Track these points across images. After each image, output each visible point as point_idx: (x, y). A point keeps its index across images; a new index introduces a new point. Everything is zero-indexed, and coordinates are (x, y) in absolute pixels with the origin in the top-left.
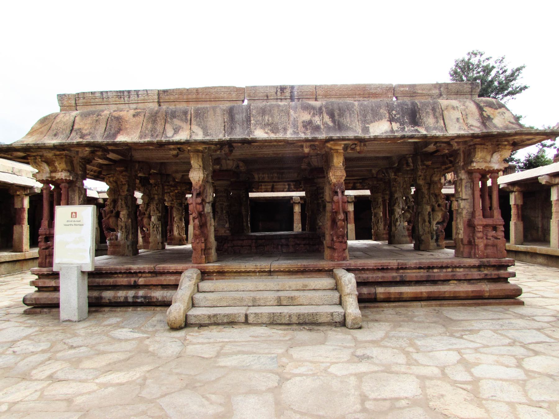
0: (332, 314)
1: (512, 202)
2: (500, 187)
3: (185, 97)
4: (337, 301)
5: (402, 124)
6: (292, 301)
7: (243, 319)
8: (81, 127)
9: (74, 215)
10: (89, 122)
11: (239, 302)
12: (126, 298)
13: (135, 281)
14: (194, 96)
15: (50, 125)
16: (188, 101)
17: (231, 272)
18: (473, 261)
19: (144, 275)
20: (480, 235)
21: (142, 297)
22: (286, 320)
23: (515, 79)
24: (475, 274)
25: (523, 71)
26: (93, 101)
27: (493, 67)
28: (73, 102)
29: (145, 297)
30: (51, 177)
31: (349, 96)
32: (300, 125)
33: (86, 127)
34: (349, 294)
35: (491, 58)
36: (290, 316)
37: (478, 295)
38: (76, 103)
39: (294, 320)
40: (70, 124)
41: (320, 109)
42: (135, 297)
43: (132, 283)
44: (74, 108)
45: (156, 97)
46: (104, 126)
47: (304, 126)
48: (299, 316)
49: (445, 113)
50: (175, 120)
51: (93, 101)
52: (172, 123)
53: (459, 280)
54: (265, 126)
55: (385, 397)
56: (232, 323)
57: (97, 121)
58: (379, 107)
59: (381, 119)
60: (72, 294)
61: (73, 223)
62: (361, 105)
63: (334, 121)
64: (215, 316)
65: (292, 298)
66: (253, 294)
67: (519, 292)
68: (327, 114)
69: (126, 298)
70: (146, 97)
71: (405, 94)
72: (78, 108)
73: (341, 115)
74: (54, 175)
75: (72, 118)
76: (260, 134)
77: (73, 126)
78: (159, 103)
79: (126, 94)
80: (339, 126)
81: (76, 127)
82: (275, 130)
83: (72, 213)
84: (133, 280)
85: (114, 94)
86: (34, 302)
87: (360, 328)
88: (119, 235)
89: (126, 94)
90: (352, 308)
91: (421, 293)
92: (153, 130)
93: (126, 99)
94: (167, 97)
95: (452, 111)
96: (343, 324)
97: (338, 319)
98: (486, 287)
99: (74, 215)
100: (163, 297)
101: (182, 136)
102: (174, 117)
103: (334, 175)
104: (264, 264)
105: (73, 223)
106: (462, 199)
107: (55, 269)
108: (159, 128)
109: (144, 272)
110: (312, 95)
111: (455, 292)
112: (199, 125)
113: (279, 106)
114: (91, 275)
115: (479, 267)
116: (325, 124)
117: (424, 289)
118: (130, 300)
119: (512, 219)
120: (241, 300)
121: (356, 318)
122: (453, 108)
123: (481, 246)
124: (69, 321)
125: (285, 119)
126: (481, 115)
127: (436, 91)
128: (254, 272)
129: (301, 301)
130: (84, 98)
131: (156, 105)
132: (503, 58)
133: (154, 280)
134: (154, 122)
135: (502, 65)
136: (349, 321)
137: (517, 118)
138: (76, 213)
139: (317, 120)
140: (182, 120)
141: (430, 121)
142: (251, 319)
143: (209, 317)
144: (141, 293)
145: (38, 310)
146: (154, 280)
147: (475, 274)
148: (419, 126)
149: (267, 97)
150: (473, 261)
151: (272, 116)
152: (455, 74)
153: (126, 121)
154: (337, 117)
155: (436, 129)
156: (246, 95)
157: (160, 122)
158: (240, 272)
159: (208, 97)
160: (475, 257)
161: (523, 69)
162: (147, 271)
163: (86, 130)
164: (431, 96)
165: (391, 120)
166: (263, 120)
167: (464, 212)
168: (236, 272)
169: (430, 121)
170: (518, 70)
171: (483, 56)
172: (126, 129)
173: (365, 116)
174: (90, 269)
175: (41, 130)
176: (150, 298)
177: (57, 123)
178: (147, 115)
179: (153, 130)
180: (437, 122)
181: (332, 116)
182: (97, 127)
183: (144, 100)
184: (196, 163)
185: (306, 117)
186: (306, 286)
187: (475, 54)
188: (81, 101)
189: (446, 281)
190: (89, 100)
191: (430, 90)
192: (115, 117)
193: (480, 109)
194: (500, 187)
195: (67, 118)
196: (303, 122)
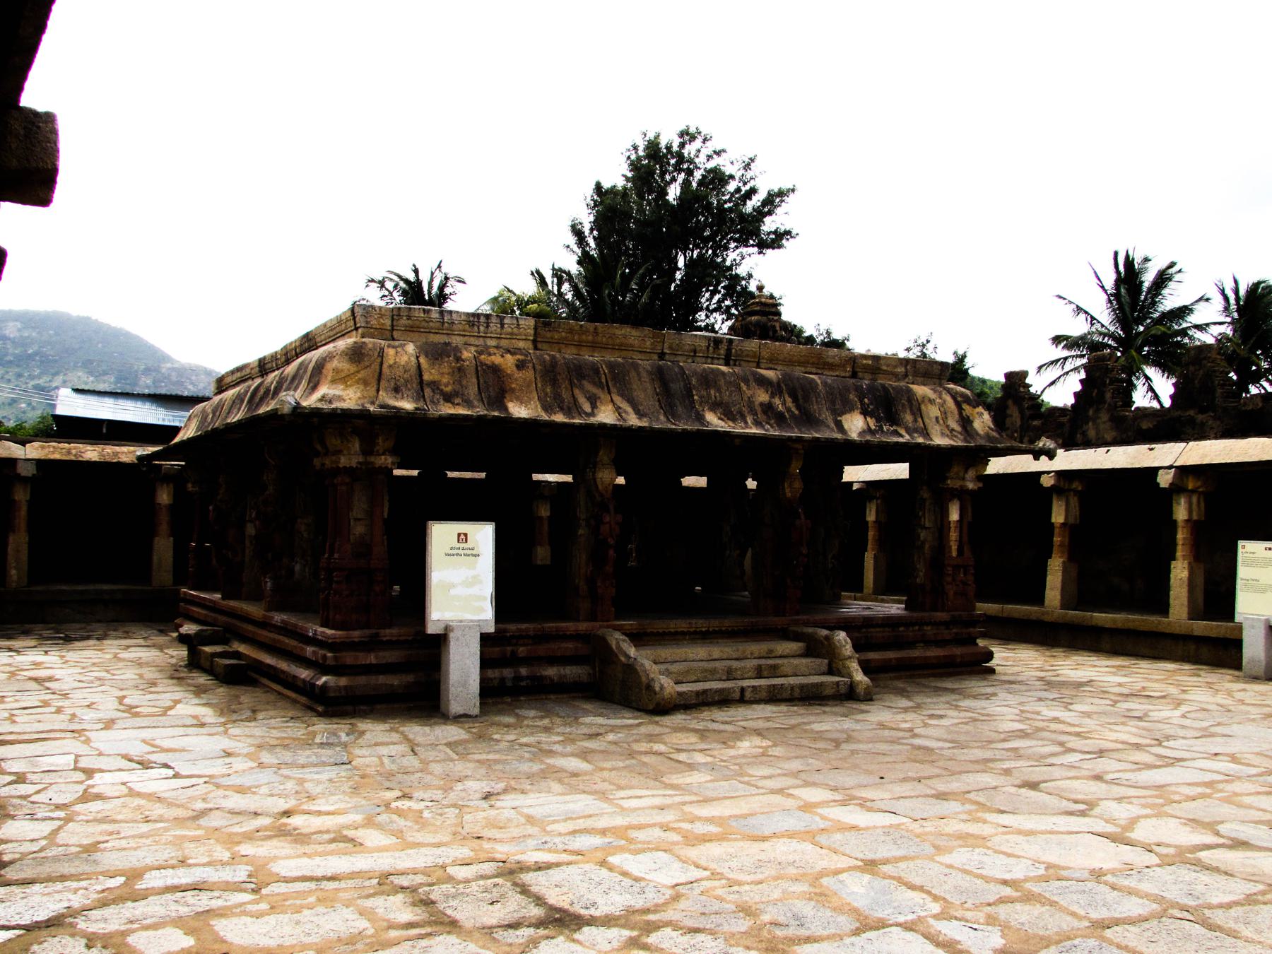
0: (837, 683)
1: (871, 517)
2: (855, 487)
3: (576, 337)
4: (825, 668)
5: (878, 421)
6: (774, 671)
7: (737, 695)
8: (437, 378)
9: (463, 537)
10: (446, 370)
11: (710, 675)
12: (503, 680)
13: (513, 652)
14: (590, 338)
15: (376, 366)
16: (579, 345)
17: (652, 634)
18: (941, 616)
19: (521, 642)
20: (949, 579)
21: (527, 677)
22: (786, 695)
23: (770, 213)
24: (946, 634)
25: (791, 199)
26: (424, 324)
27: (732, 177)
28: (388, 322)
29: (532, 678)
30: (367, 463)
31: (800, 364)
32: (759, 409)
33: (445, 380)
34: (850, 657)
35: (724, 151)
36: (792, 688)
37: (657, 719)
38: (392, 326)
39: (797, 693)
40: (413, 370)
41: (778, 383)
42: (518, 678)
43: (508, 654)
44: (388, 334)
45: (532, 332)
46: (475, 380)
47: (765, 412)
48: (802, 687)
49: (923, 407)
50: (585, 383)
51: (424, 324)
52: (582, 388)
53: (928, 643)
54: (714, 407)
55: (648, 905)
56: (723, 700)
57: (460, 369)
58: (848, 390)
59: (851, 410)
60: (463, 670)
61: (461, 552)
62: (825, 384)
63: (798, 407)
64: (705, 692)
65: (774, 667)
66: (728, 663)
67: (990, 656)
68: (790, 396)
69: (503, 680)
70: (515, 330)
71: (867, 369)
72: (396, 334)
73: (807, 398)
74: (372, 459)
75: (413, 359)
76: (714, 421)
77: (421, 375)
78: (535, 342)
79: (482, 319)
80: (808, 419)
81: (426, 377)
82: (728, 415)
83: (459, 535)
84: (509, 649)
85: (463, 317)
86: (343, 693)
87: (871, 700)
88: (297, 568)
89: (482, 319)
90: (859, 676)
91: (890, 660)
92: (557, 396)
93: (482, 329)
94: (549, 335)
95: (930, 407)
96: (849, 696)
97: (843, 690)
98: (958, 651)
99: (463, 537)
100: (561, 677)
101: (606, 416)
102: (582, 376)
103: (790, 486)
104: (701, 624)
105: (461, 552)
106: (924, 528)
107: (432, 629)
108: (565, 395)
109: (528, 637)
110: (754, 356)
111: (926, 658)
112: (622, 396)
113: (723, 373)
114: (485, 639)
115: (947, 624)
116: (789, 410)
117: (891, 655)
118: (509, 684)
119: (870, 546)
120: (713, 671)
121: (868, 687)
122: (931, 401)
123: (951, 593)
124: (466, 716)
125: (736, 397)
126: (960, 414)
127: (901, 370)
128: (683, 633)
129: (788, 670)
130: (409, 318)
131: (529, 345)
132: (752, 160)
133: (542, 650)
134: (554, 382)
135: (749, 174)
136: (860, 690)
137: (828, 333)
138: (466, 535)
139: (777, 401)
140: (594, 384)
141: (908, 418)
142: (748, 695)
143: (698, 693)
144: (524, 671)
145: (349, 708)
146: (542, 650)
147: (946, 634)
148: (898, 425)
149: (695, 351)
150: (941, 616)
151: (719, 390)
152: (635, 166)
153: (509, 376)
154: (801, 401)
155: (916, 430)
156: (666, 345)
157: (564, 385)
158: (670, 634)
159: (611, 342)
160: (943, 611)
161: (791, 195)
162: (531, 633)
163: (446, 385)
164: (895, 375)
165: (865, 413)
166: (709, 395)
167: (927, 546)
168: (658, 634)
169: (908, 418)
170: (781, 194)
171: (708, 144)
172: (513, 390)
173: (833, 403)
174: (491, 629)
175: (359, 376)
176: (542, 678)
177: (390, 366)
178: (539, 367)
179: (557, 396)
180: (915, 421)
181: (795, 400)
182: (464, 383)
183: (511, 334)
184: (604, 456)
185: (763, 397)
186: (771, 651)
187: (693, 138)
188: (404, 321)
189: (911, 645)
190: (417, 323)
191: (896, 367)
192: (489, 367)
193: (958, 404)
194: (855, 487)
195: (404, 359)
196: (761, 404)
